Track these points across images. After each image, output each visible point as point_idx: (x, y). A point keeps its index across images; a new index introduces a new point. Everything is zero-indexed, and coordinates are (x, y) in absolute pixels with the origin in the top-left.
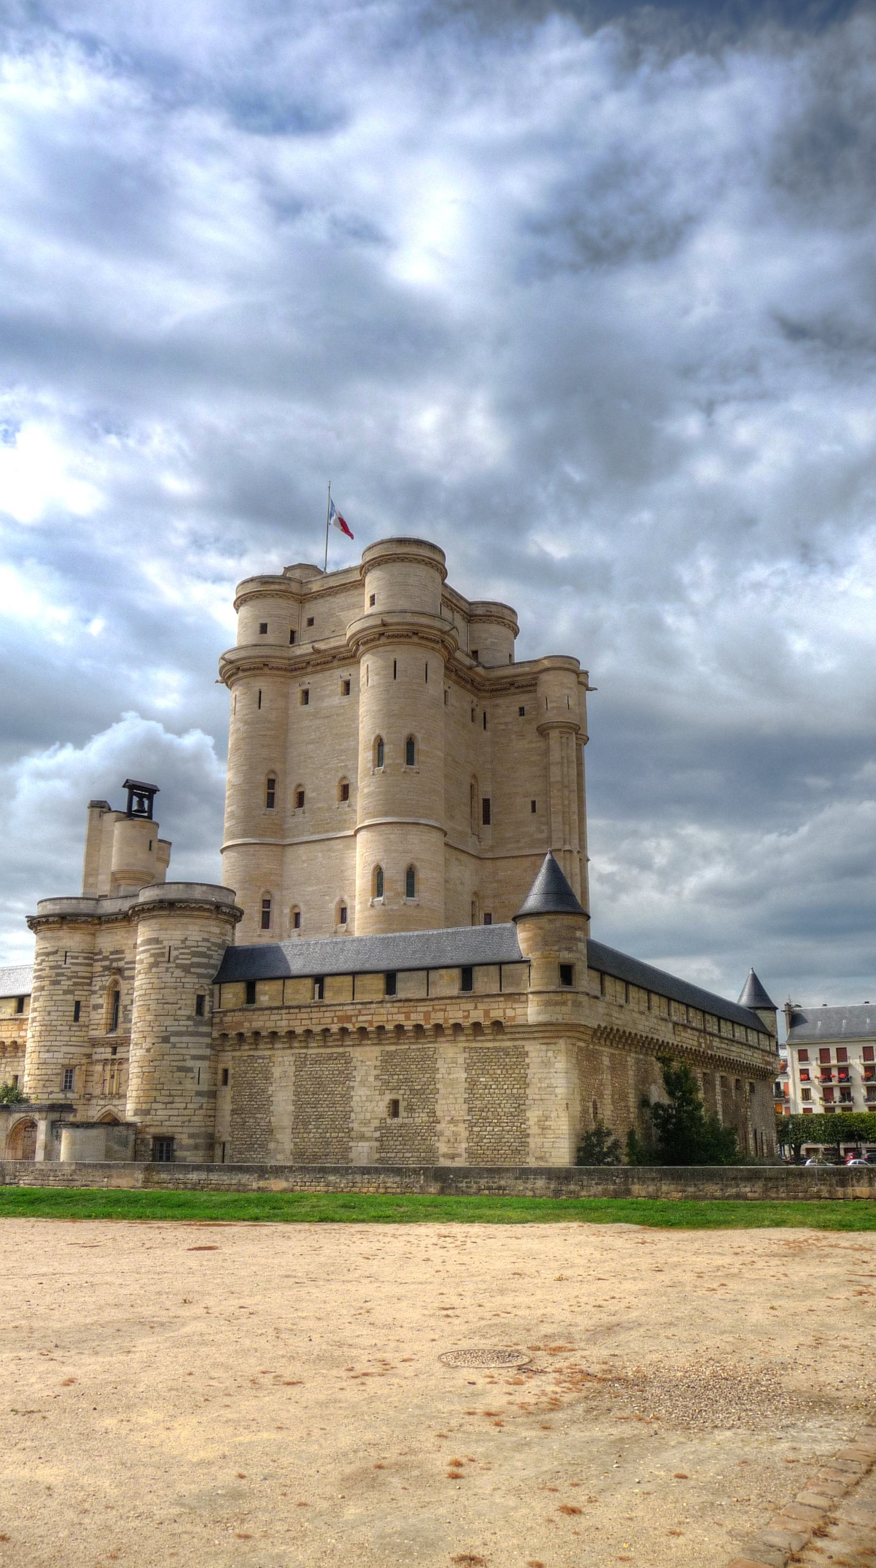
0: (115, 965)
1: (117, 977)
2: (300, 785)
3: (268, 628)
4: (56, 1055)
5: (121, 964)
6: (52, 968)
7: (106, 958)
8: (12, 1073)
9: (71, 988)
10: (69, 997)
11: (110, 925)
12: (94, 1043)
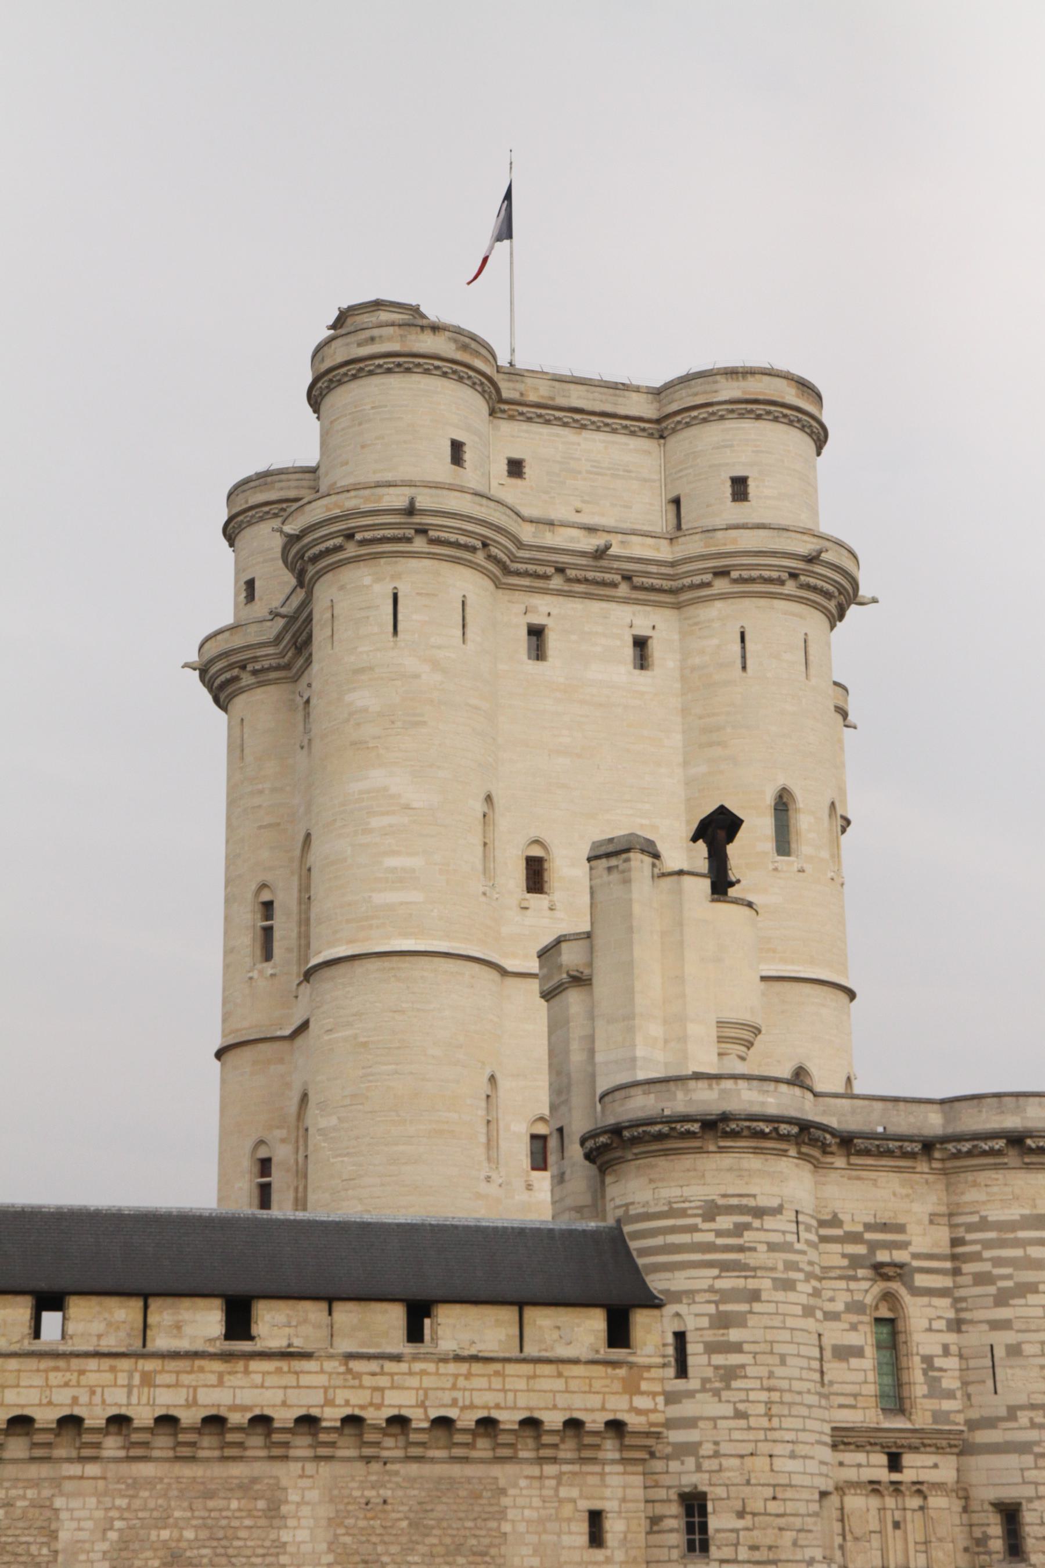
0: (882, 1256)
1: (895, 1286)
2: (537, 842)
3: (468, 456)
4: (812, 1466)
5: (900, 1256)
6: (772, 1247)
7: (854, 1238)
8: (586, 1505)
9: (812, 1301)
10: (810, 1324)
11: (870, 1161)
12: (843, 1439)
